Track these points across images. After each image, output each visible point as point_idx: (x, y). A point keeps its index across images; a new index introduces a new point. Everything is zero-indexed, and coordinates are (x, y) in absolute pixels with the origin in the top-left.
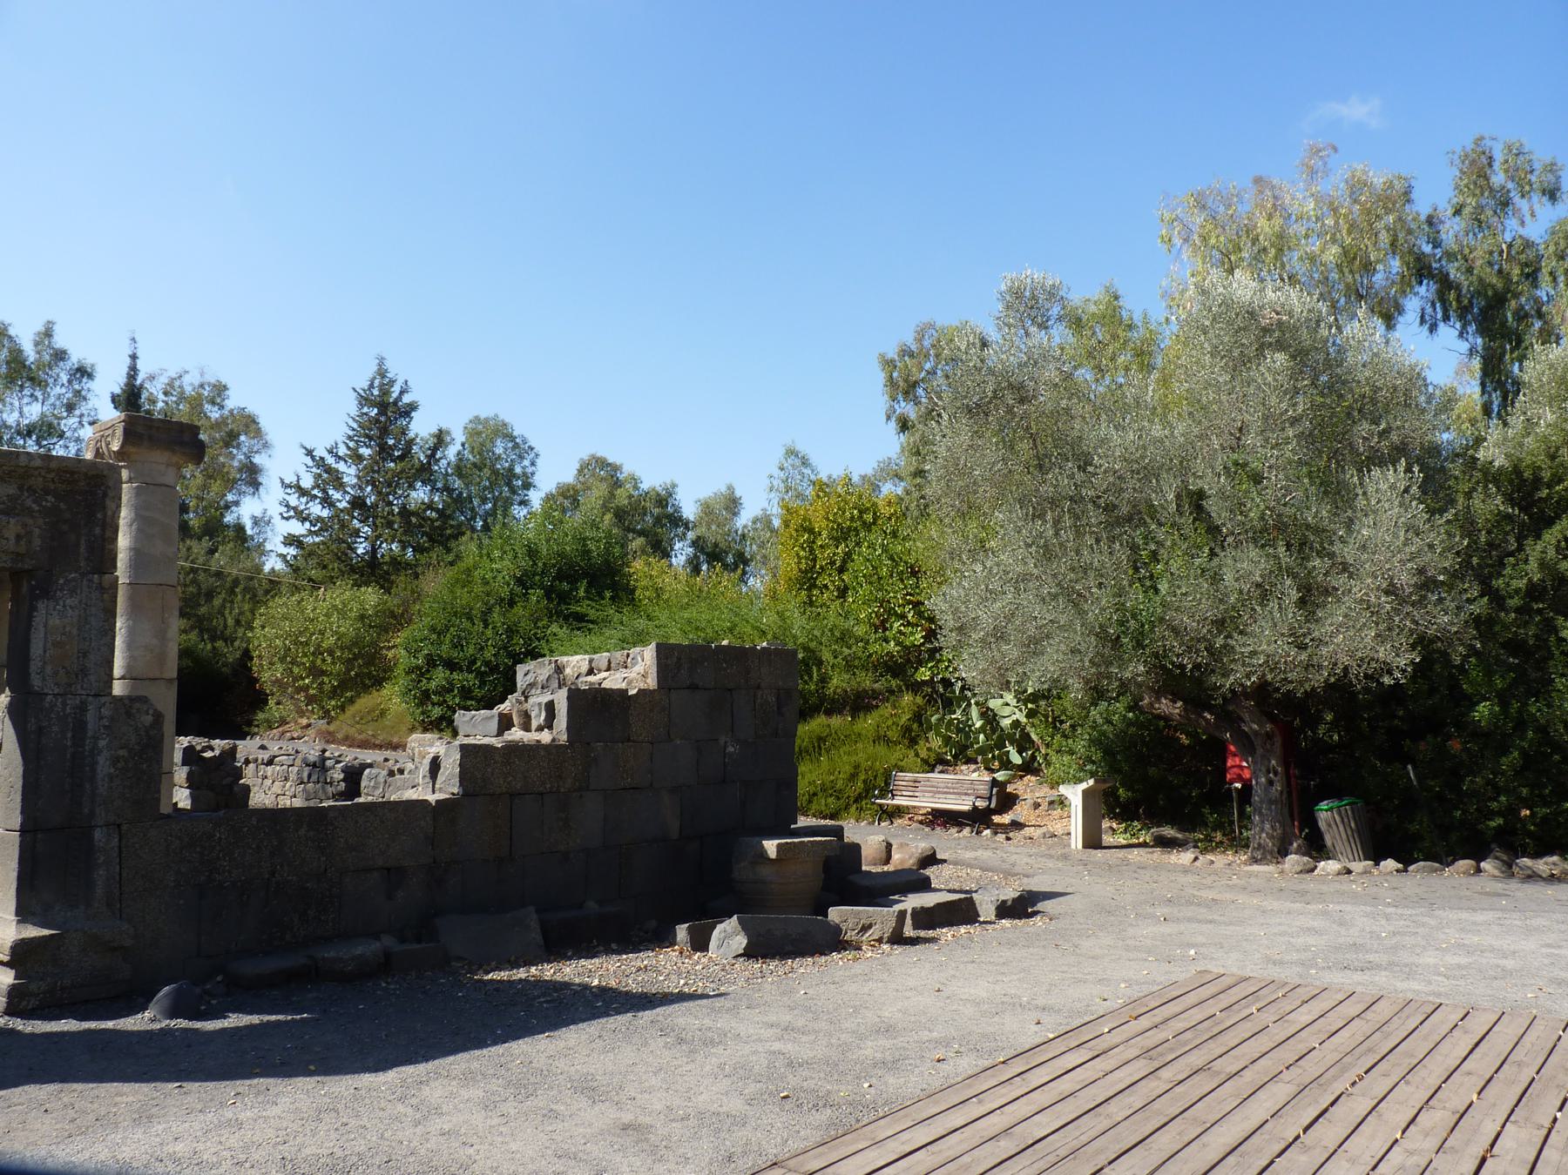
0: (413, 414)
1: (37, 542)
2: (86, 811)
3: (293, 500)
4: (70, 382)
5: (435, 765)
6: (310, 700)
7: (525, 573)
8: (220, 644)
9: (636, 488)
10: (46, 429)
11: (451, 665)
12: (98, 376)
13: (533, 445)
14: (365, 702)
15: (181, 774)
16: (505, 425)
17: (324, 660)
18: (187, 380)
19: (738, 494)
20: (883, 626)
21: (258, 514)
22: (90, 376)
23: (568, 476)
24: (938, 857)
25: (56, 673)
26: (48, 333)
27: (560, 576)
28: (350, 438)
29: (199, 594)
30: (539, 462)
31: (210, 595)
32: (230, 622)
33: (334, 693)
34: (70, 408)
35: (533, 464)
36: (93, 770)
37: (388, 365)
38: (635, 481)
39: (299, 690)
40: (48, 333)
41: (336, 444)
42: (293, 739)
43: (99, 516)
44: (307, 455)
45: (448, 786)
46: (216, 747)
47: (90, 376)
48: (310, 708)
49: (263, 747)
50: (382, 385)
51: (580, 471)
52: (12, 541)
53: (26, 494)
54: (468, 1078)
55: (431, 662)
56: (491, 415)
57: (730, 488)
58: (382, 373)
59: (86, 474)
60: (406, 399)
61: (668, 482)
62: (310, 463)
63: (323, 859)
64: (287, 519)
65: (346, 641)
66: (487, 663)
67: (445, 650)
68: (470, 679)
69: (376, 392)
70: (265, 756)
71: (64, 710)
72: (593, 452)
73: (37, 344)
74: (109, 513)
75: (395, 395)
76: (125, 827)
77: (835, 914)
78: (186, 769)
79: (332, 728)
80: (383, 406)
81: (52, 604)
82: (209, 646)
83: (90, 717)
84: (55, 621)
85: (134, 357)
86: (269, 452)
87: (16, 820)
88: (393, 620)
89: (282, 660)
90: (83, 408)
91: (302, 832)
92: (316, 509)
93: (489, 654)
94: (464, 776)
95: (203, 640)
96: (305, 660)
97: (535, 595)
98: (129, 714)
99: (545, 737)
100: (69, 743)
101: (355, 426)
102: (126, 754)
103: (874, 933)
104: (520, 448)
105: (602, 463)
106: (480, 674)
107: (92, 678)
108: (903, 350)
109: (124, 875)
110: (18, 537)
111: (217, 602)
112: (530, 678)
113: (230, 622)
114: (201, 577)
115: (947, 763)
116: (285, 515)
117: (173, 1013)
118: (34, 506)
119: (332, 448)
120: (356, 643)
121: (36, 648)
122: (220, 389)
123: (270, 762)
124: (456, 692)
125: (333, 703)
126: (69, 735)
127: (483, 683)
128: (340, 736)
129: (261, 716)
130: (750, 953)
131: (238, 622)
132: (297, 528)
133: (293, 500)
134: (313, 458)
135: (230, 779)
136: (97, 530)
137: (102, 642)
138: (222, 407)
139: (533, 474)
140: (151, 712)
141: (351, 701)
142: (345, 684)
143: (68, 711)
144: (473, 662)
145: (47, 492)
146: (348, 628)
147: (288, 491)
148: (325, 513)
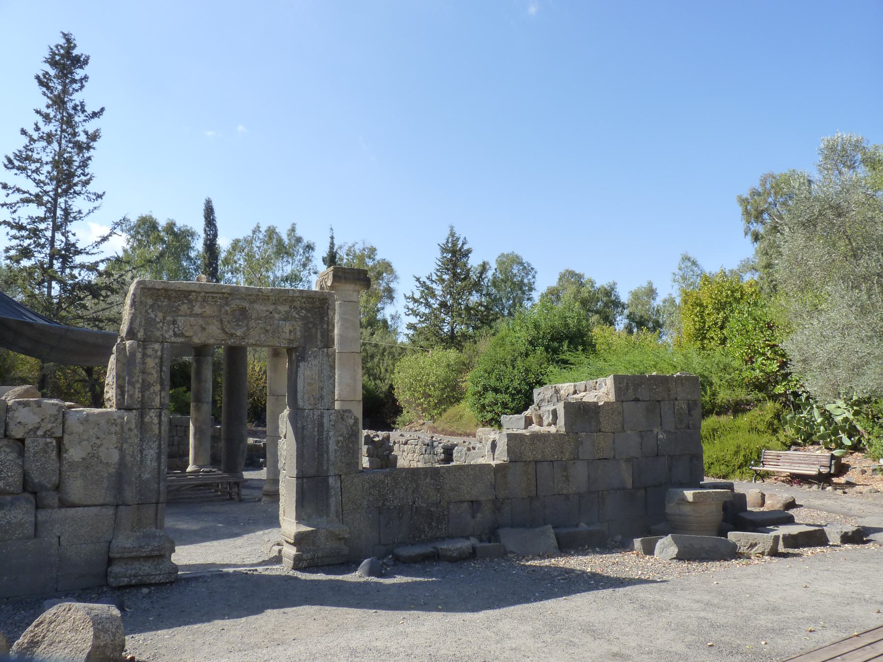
0: (469, 255)
1: (299, 334)
2: (325, 468)
3: (411, 305)
4: (304, 253)
5: (494, 445)
6: (424, 410)
7: (534, 338)
8: (378, 382)
9: (593, 286)
10: (294, 278)
11: (496, 390)
12: (317, 248)
13: (533, 267)
14: (452, 411)
15: (364, 449)
16: (517, 257)
17: (430, 389)
18: (357, 247)
19: (654, 287)
20: (751, 360)
21: (393, 313)
22: (313, 249)
23: (554, 282)
24: (797, 503)
25: (309, 398)
26: (293, 230)
27: (553, 339)
28: (438, 270)
29: (367, 356)
30: (537, 276)
31: (372, 357)
32: (383, 370)
33: (436, 406)
34: (304, 265)
35: (534, 277)
36: (327, 447)
37: (456, 230)
38: (592, 283)
39: (418, 405)
40: (293, 230)
41: (431, 274)
42: (416, 431)
43: (326, 319)
44: (417, 281)
45: (501, 457)
46: (380, 435)
48: (424, 414)
49: (402, 435)
50: (453, 241)
51: (560, 279)
52: (288, 334)
53: (293, 310)
54: (523, 619)
55: (485, 389)
56: (510, 252)
57: (650, 283)
58: (452, 234)
59: (319, 298)
60: (466, 247)
61: (611, 282)
62: (419, 285)
63: (439, 495)
64: (408, 315)
65: (441, 379)
66: (515, 389)
67: (493, 382)
68: (507, 398)
69: (450, 245)
70: (403, 440)
71: (313, 417)
72: (566, 268)
73: (289, 235)
74: (330, 317)
75: (459, 246)
76: (343, 477)
77: (732, 536)
78: (366, 447)
79: (435, 425)
80: (454, 252)
81: (306, 364)
82: (373, 383)
83: (325, 420)
84: (308, 373)
85: (332, 238)
86: (398, 281)
87: (294, 473)
88: (465, 367)
89: (409, 389)
90: (310, 266)
91: (428, 480)
92: (423, 309)
93: (516, 384)
94: (510, 451)
95: (370, 380)
96: (420, 389)
97: (540, 350)
98: (343, 419)
99: (553, 429)
100: (316, 434)
101: (440, 264)
102: (342, 439)
103: (758, 549)
104: (527, 269)
105: (572, 274)
106: (512, 395)
107: (326, 400)
108: (753, 192)
109: (343, 501)
110: (290, 331)
111: (376, 360)
112: (541, 397)
113: (383, 370)
114: (368, 347)
115: (798, 444)
116: (407, 313)
117: (371, 573)
118: (296, 316)
119: (429, 276)
121: (300, 387)
122: (373, 250)
123: (406, 443)
124: (499, 404)
125: (436, 412)
126: (316, 430)
127: (513, 400)
128: (440, 429)
129: (399, 419)
130: (680, 557)
131: (386, 370)
132: (413, 320)
133: (411, 305)
134: (420, 282)
135: (388, 452)
136: (325, 326)
137: (330, 382)
138: (374, 260)
139: (534, 283)
140: (353, 417)
141: (445, 410)
142: (440, 402)
143: (315, 417)
144: (508, 388)
145: (302, 308)
146: (442, 372)
147: (408, 300)
148: (427, 311)
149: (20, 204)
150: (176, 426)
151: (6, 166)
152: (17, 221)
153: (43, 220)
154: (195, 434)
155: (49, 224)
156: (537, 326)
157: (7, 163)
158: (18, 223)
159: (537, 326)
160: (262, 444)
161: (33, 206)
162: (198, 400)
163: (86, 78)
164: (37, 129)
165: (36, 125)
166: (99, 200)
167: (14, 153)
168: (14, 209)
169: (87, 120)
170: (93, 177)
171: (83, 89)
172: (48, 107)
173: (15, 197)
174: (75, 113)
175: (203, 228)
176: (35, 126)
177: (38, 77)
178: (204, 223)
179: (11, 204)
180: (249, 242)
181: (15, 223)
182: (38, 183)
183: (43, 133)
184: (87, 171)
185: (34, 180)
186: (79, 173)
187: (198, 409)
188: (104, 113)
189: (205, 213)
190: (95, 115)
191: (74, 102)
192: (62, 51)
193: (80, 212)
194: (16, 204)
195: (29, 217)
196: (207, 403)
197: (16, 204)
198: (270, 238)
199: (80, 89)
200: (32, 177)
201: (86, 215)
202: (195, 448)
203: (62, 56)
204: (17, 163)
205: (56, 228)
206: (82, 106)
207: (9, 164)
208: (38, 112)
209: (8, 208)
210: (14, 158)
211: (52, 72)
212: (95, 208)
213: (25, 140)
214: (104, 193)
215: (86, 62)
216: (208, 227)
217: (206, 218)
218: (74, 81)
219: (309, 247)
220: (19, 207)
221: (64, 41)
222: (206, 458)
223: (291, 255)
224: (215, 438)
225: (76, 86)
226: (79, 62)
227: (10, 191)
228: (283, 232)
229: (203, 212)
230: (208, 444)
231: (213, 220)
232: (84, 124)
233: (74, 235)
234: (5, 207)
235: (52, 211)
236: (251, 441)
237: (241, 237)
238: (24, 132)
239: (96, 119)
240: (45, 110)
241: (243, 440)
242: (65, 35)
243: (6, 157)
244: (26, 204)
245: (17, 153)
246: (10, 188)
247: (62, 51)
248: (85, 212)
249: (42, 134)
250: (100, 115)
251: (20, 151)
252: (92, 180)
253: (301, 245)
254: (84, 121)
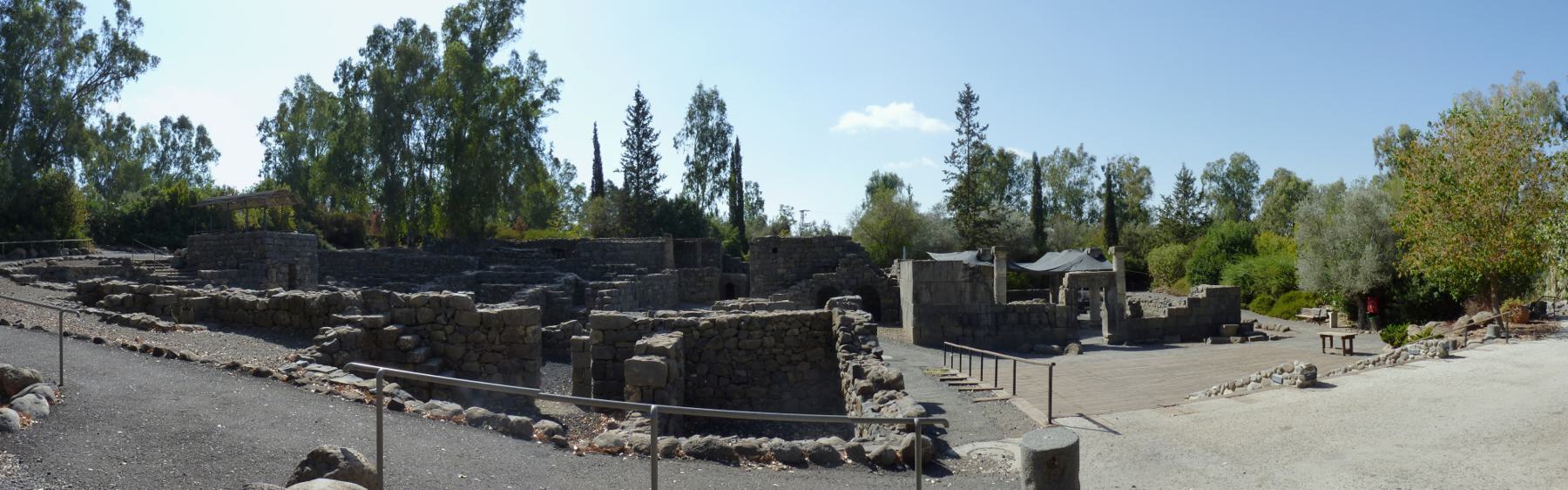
8: (1140, 259)
10: (1082, 182)
12: (1097, 160)
14: (1180, 281)
22: (1094, 160)
26: (1081, 148)
27: (1231, 245)
33: (1171, 279)
34: (1089, 172)
40: (1081, 148)
47: (1094, 160)
55: (1194, 271)
73: (1078, 151)
80: (1185, 180)
90: (1092, 171)
97: (1224, 251)
120: (1176, 263)
129: (1152, 284)
146: (1173, 259)
156: (1223, 237)
159: (1223, 237)
180: (1053, 159)
198: (1066, 156)
219: (1093, 159)
223: (1080, 165)
228: (1074, 151)
237: (1047, 156)
253: (1087, 158)
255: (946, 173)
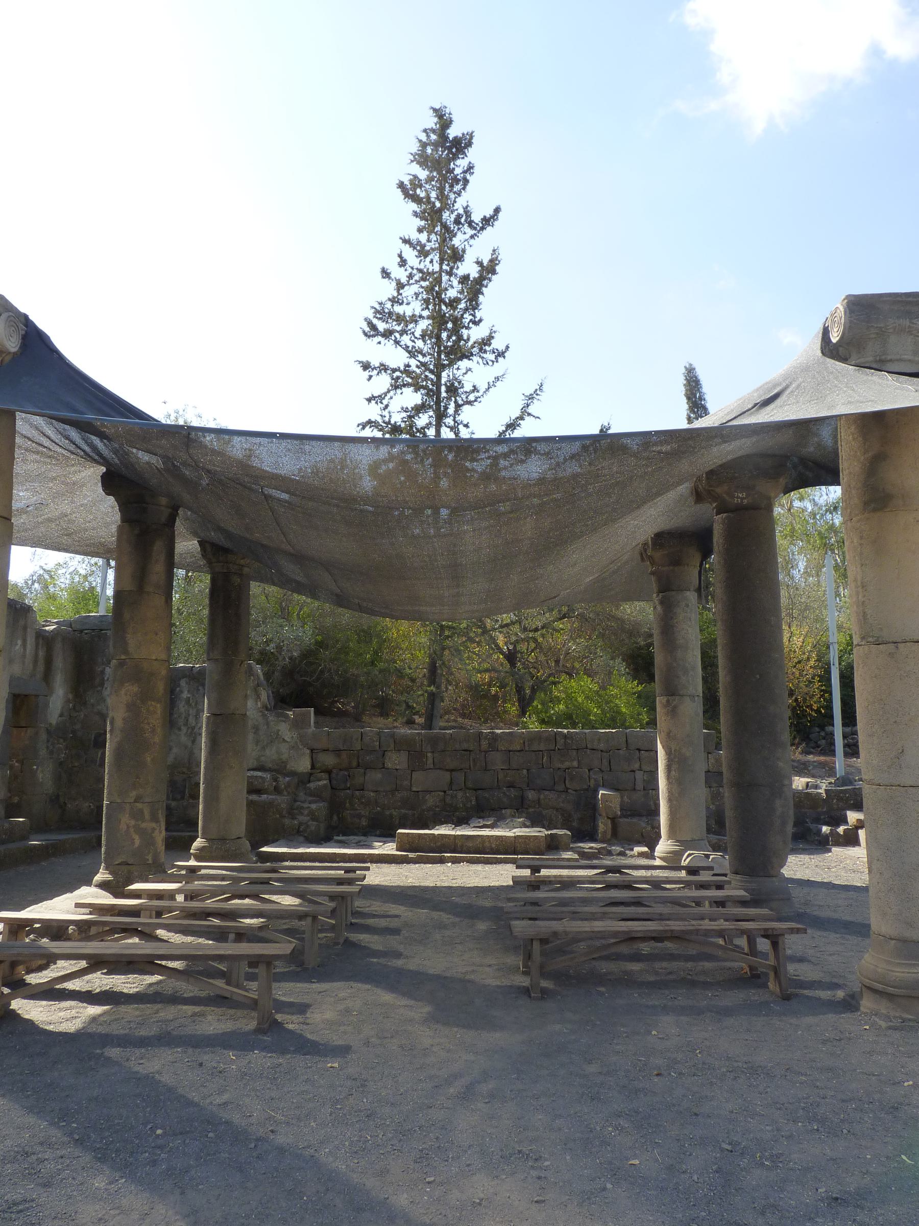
149: (392, 393)
150: (639, 750)
151: (365, 334)
152: (387, 419)
153: (419, 409)
154: (669, 768)
155: (432, 416)
157: (367, 329)
158: (389, 423)
160: (822, 791)
161: (408, 391)
162: (671, 691)
163: (470, 169)
164: (403, 263)
165: (400, 256)
166: (500, 359)
167: (373, 307)
168: (385, 402)
169: (475, 235)
170: (495, 332)
171: (468, 187)
172: (420, 230)
173: (383, 382)
174: (459, 229)
175: (685, 416)
176: (399, 260)
177: (401, 185)
178: (686, 407)
179: (379, 396)
181: (384, 422)
182: (412, 353)
183: (412, 268)
184: (479, 315)
185: (406, 348)
186: (467, 321)
187: (673, 711)
188: (500, 215)
189: (686, 390)
190: (487, 221)
191: (456, 213)
192: (434, 137)
193: (475, 389)
194: (386, 394)
195: (402, 408)
196: (692, 697)
197: (386, 394)
199: (464, 189)
200: (402, 343)
201: (485, 392)
202: (670, 800)
203: (436, 145)
204: (381, 326)
205: (440, 416)
206: (466, 210)
207: (372, 331)
208: (406, 241)
209: (377, 403)
210: (374, 317)
211: (423, 174)
212: (497, 379)
213: (389, 289)
214: (507, 347)
215: (469, 144)
216: (694, 412)
217: (688, 398)
218: (456, 181)
220: (391, 398)
221: (436, 120)
222: (697, 825)
224: (713, 777)
225: (457, 188)
226: (460, 146)
227: (375, 372)
229: (683, 389)
230: (700, 793)
231: (701, 399)
232: (472, 242)
233: (466, 426)
234: (373, 402)
235: (433, 393)
236: (799, 783)
238: (385, 274)
239: (489, 228)
240: (414, 236)
241: (779, 784)
242: (435, 110)
243: (366, 319)
244: (399, 391)
245: (379, 308)
246: (375, 368)
247: (434, 137)
248: (482, 387)
249: (410, 270)
250: (494, 220)
251: (380, 304)
252: (493, 337)
254: (472, 237)
255: (366, 366)
